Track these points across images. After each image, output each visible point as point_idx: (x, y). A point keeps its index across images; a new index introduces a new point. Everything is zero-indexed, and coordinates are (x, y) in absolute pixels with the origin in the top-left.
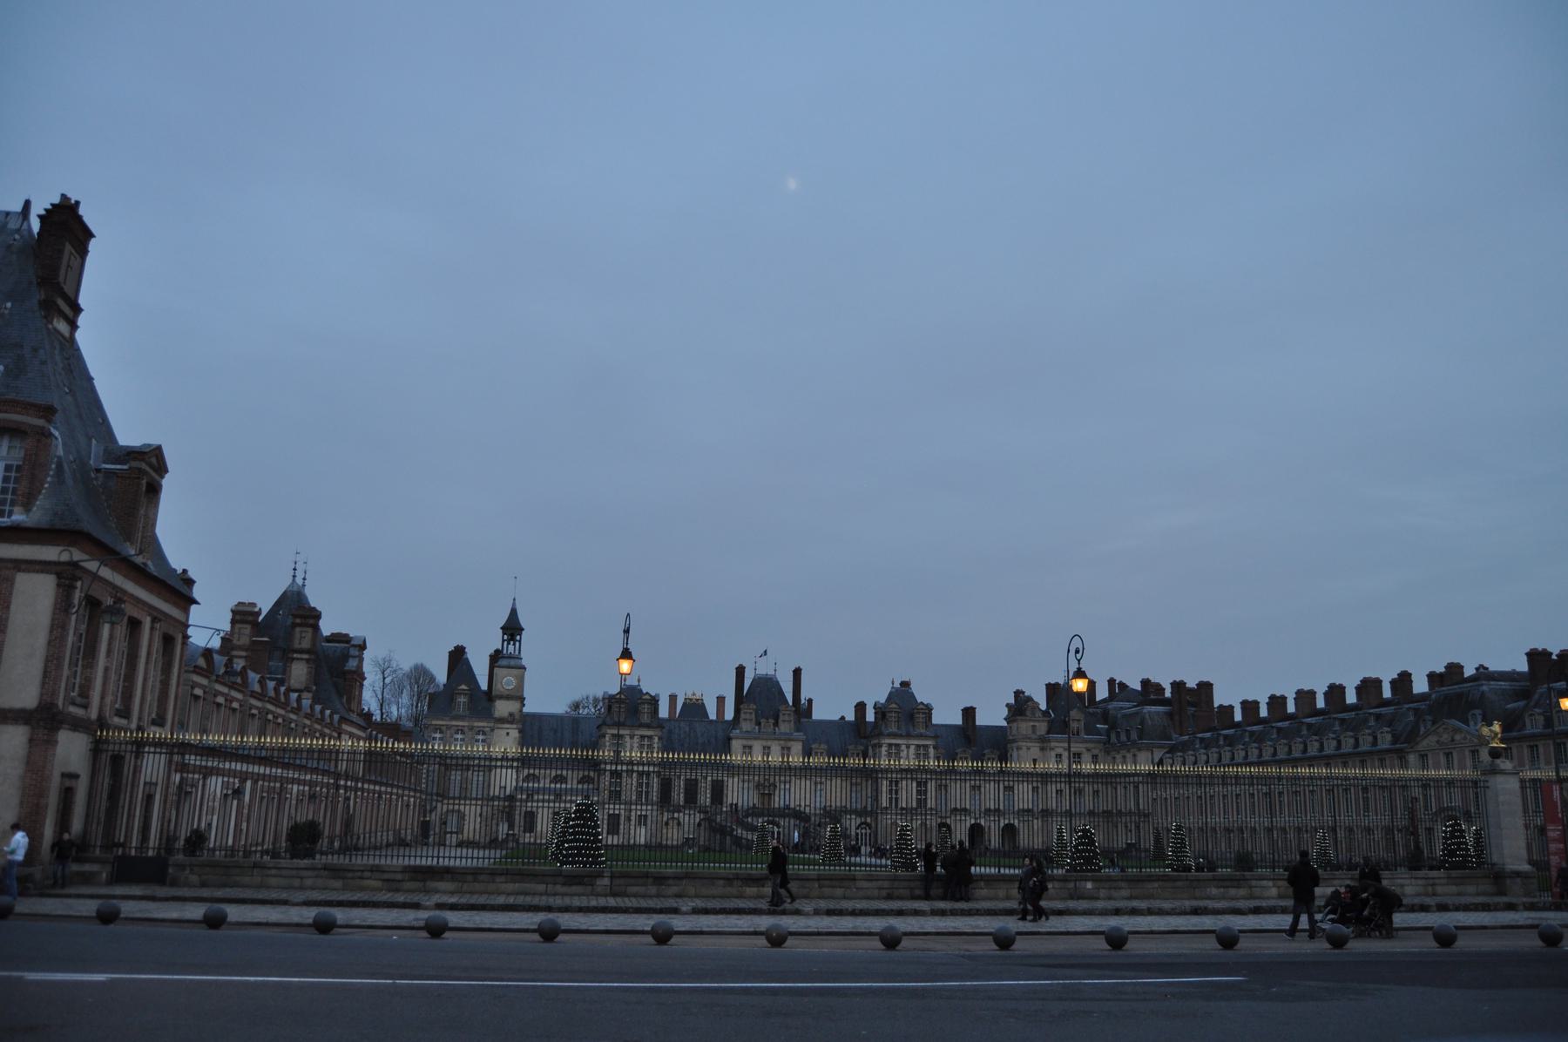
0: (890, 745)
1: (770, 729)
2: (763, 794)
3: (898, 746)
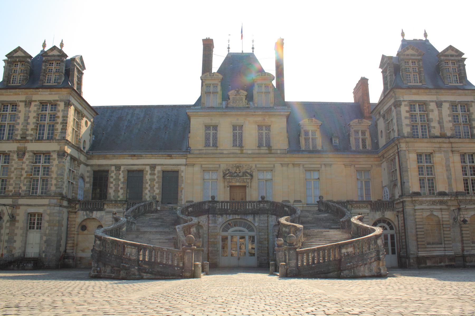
0: (412, 104)
1: (244, 103)
2: (231, 187)
3: (423, 104)
